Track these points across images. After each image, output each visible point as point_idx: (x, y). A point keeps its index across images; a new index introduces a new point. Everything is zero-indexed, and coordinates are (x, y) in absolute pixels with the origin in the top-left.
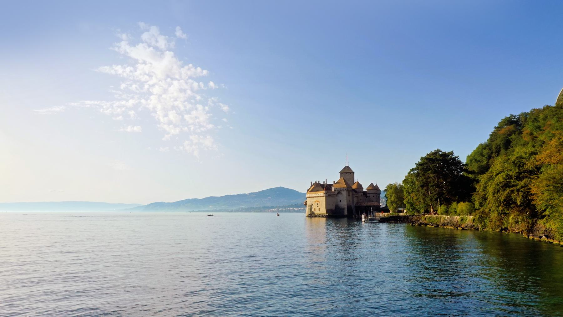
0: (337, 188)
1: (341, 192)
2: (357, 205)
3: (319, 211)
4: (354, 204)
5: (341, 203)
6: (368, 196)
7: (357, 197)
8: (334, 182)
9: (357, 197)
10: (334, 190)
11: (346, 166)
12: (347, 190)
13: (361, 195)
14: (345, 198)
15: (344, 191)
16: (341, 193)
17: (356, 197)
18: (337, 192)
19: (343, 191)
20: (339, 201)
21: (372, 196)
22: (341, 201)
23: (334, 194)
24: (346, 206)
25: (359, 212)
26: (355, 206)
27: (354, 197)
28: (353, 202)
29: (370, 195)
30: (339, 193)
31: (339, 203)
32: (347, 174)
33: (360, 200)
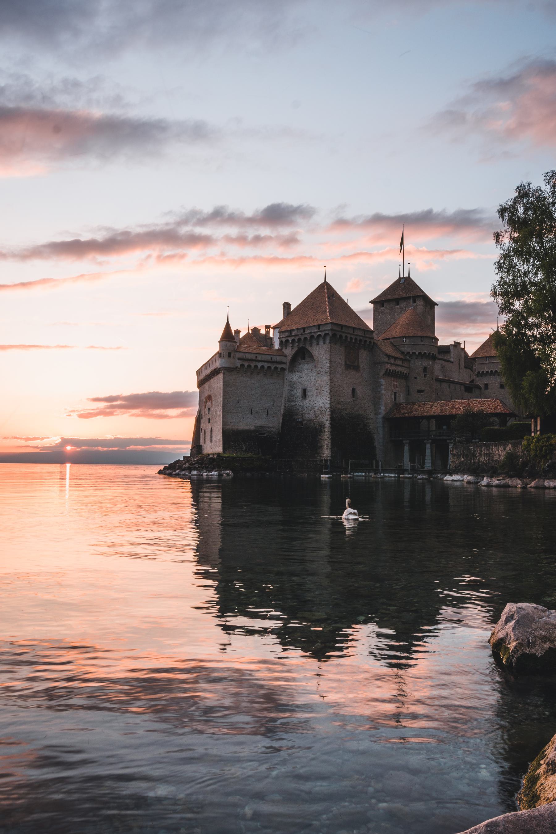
0: (290, 331)
1: (310, 349)
2: (397, 415)
3: (211, 441)
4: (383, 410)
5: (307, 403)
6: (480, 388)
7: (404, 377)
8: (287, 306)
9: (404, 377)
10: (281, 343)
11: (402, 276)
12: (334, 335)
13: (425, 369)
14: (326, 379)
15: (321, 342)
16: (311, 356)
17: (389, 374)
18: (289, 352)
19: (315, 342)
20: (299, 392)
21: (498, 384)
22: (309, 394)
23: (278, 359)
24: (328, 412)
25: (406, 448)
26: (387, 419)
27: (382, 373)
28: (376, 401)
29: (487, 380)
30: (304, 359)
31: (299, 402)
32: (403, 304)
33: (420, 391)
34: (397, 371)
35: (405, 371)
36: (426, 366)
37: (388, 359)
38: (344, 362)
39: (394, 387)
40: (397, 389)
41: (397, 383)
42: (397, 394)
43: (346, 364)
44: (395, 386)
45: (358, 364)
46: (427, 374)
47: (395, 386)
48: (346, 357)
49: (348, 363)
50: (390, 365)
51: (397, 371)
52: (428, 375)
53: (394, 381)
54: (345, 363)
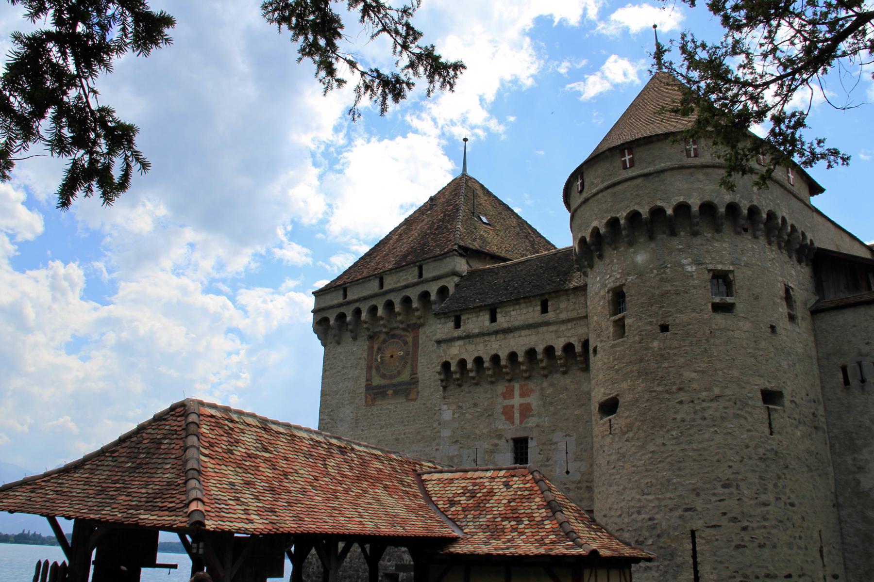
34: (503, 355)
35: (572, 335)
36: (618, 284)
37: (451, 324)
38: (364, 385)
39: (510, 418)
40: (532, 422)
41: (533, 400)
42: (531, 444)
43: (368, 387)
44: (517, 415)
45: (414, 372)
46: (624, 317)
47: (517, 415)
48: (369, 368)
49: (377, 381)
50: (460, 343)
51: (503, 355)
52: (628, 321)
53: (508, 394)
54: (367, 385)
